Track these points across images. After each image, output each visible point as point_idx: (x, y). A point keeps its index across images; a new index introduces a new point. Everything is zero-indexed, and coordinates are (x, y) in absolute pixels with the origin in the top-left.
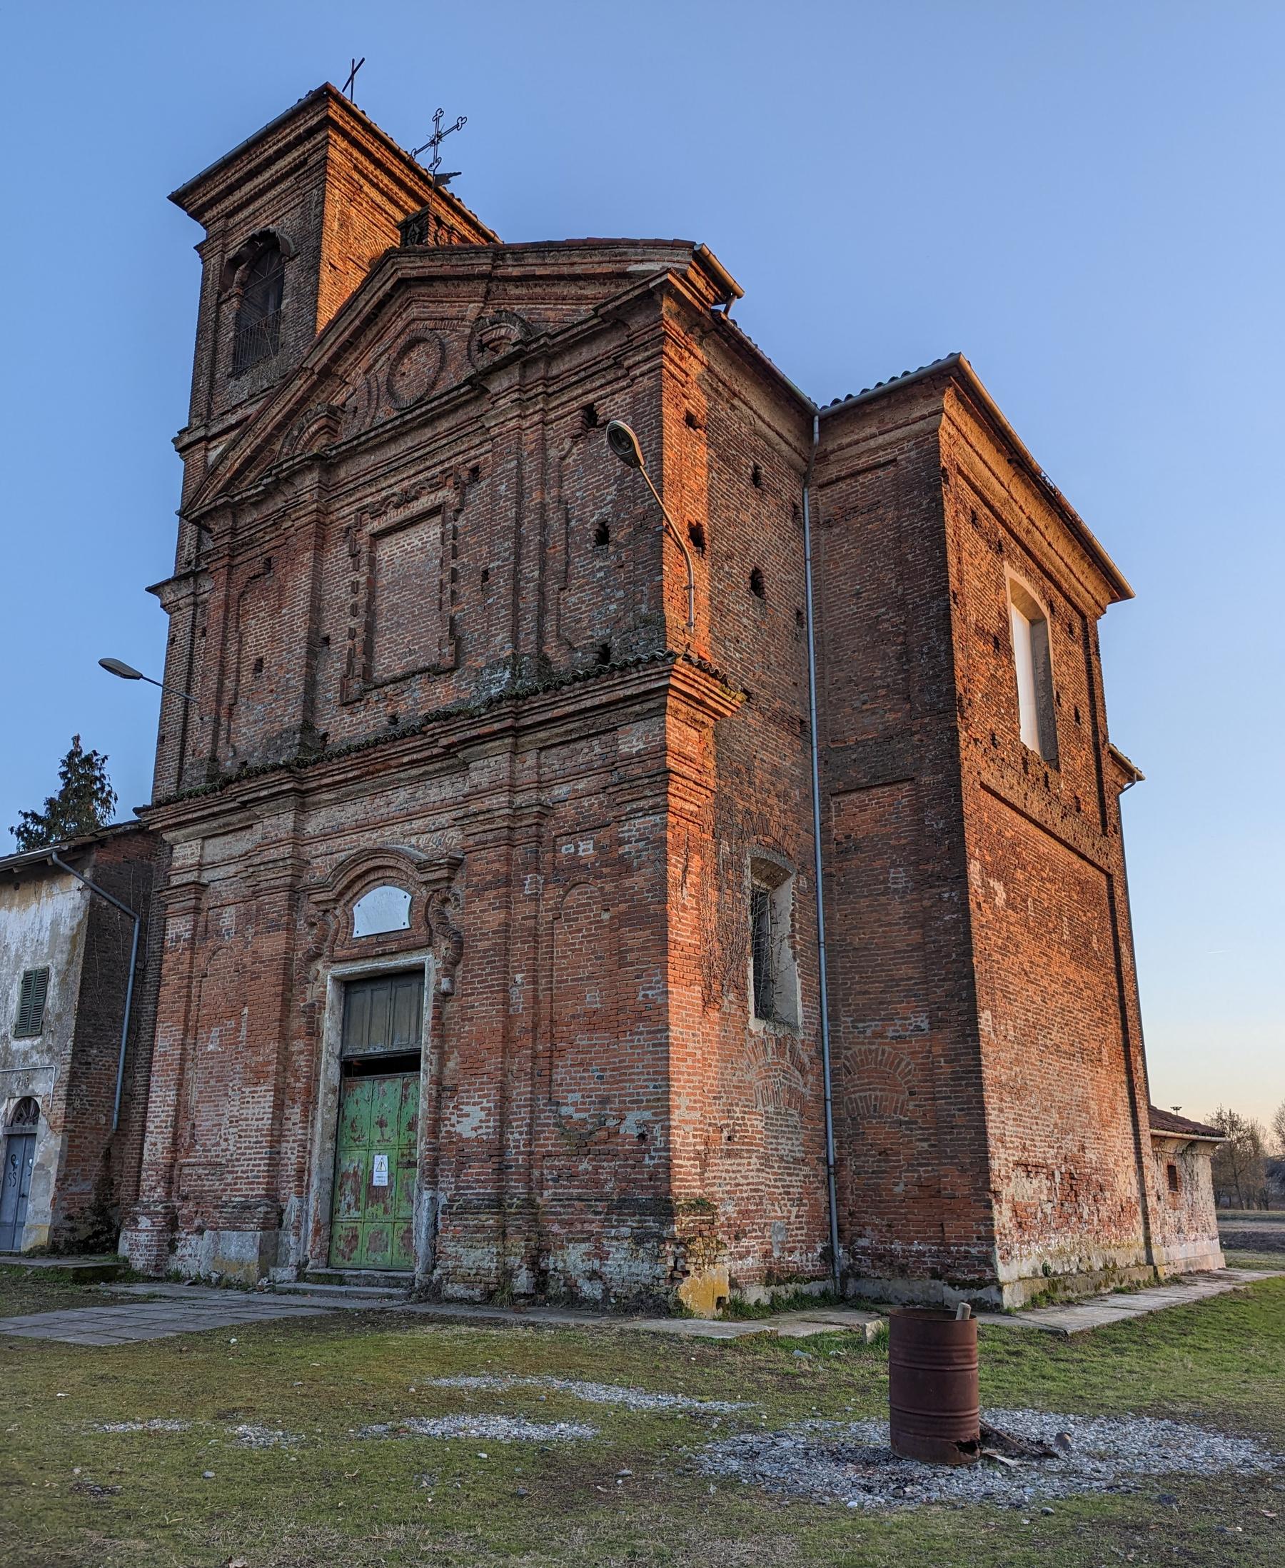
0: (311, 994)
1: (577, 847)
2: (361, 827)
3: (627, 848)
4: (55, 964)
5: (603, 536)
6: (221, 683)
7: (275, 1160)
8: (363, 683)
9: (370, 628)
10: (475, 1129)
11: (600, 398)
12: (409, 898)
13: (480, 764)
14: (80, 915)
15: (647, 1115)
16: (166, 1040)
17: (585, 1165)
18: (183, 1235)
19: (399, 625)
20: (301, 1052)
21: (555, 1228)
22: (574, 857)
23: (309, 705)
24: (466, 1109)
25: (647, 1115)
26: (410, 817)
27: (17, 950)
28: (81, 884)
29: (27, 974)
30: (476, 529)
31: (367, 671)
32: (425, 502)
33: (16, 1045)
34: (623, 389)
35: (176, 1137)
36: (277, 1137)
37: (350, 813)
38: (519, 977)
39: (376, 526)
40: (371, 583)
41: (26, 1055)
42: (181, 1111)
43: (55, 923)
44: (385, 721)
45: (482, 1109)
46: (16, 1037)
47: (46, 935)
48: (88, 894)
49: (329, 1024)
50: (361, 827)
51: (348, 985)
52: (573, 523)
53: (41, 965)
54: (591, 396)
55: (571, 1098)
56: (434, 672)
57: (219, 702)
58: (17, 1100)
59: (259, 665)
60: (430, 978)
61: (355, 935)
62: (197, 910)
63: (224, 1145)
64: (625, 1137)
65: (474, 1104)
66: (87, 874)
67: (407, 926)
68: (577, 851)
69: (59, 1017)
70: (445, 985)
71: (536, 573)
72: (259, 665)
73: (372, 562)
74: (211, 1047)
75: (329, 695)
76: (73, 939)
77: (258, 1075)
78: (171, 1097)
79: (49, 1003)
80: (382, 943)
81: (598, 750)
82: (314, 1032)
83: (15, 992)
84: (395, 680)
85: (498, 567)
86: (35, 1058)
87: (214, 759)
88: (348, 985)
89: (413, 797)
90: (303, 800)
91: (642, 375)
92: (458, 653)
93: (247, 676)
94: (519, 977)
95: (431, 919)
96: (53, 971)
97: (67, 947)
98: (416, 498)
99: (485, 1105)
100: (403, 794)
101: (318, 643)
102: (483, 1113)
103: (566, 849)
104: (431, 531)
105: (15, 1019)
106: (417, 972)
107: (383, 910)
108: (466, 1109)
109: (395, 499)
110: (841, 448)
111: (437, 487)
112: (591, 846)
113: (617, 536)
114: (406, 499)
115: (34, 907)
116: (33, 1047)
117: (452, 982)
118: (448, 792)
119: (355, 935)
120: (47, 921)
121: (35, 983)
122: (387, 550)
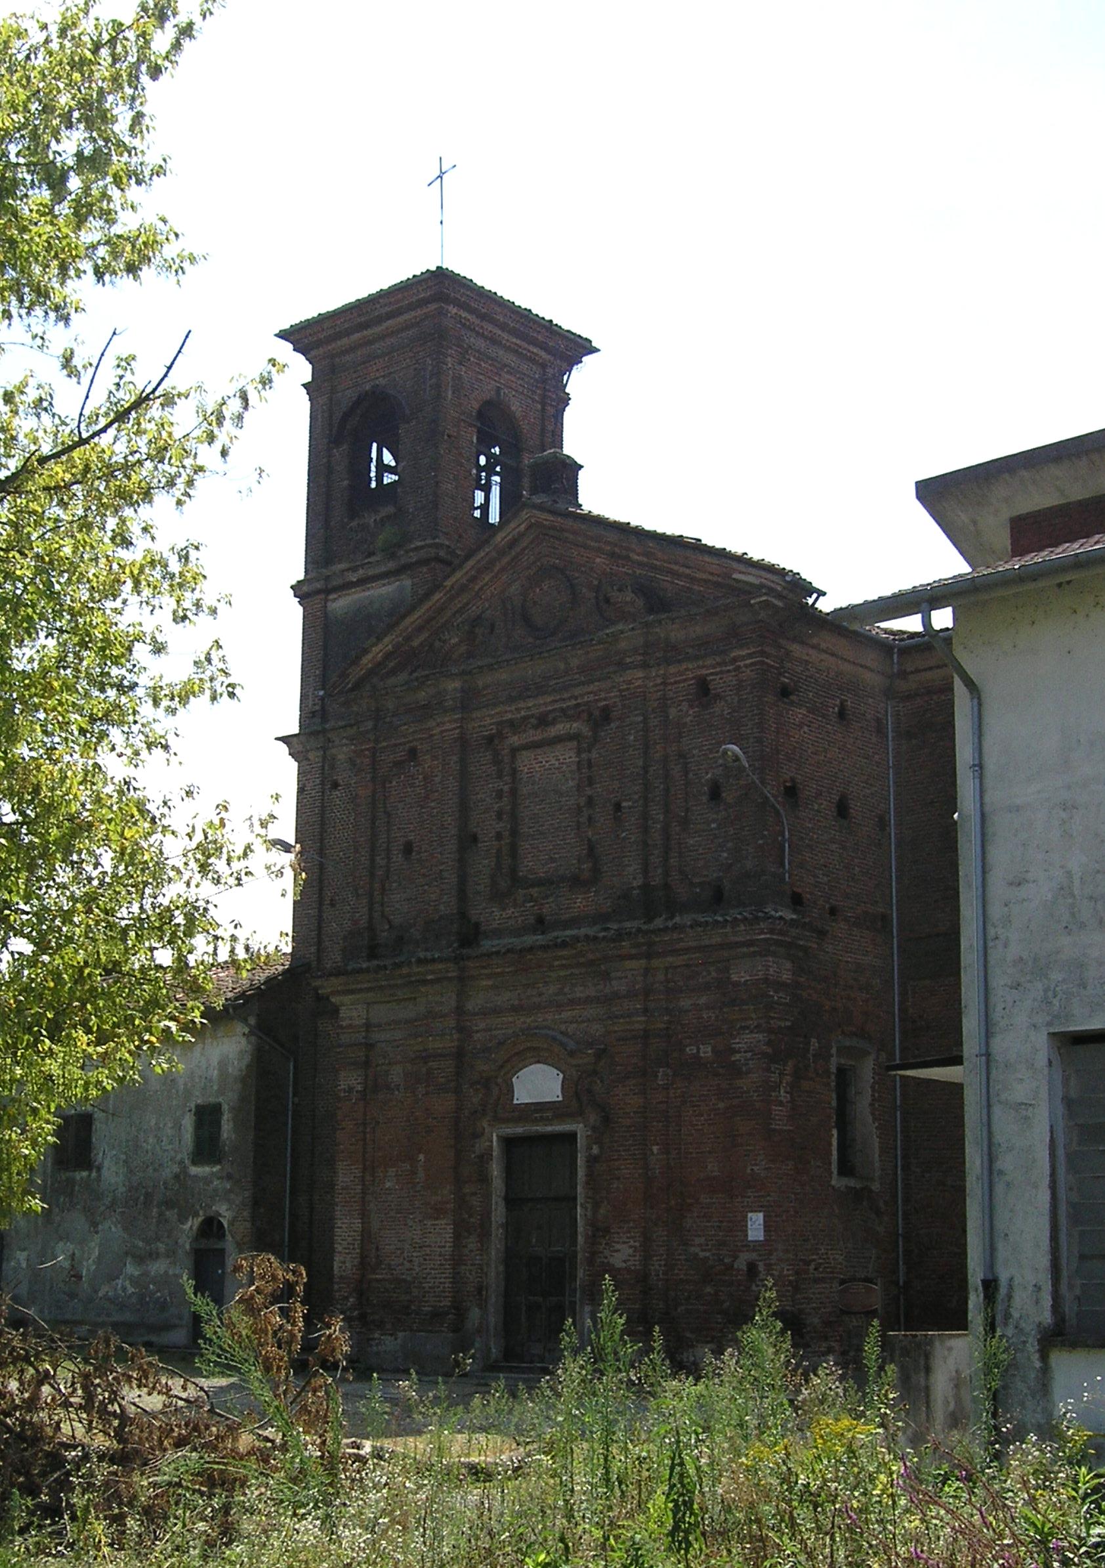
0: (480, 1146)
1: (698, 1049)
2: (515, 1009)
3: (738, 1056)
4: (228, 1102)
5: (715, 793)
6: (372, 861)
9: (514, 833)
10: (625, 1261)
11: (712, 674)
12: (561, 1076)
13: (619, 974)
14: (247, 1059)
15: (754, 1256)
16: (346, 1176)
17: (709, 1289)
18: (376, 1336)
20: (475, 1194)
21: (688, 1335)
22: (696, 1057)
23: (462, 895)
24: (618, 1246)
25: (754, 1256)
27: (185, 1084)
28: (246, 1030)
29: (197, 1106)
31: (513, 871)
32: (560, 728)
33: (194, 1170)
34: (729, 671)
35: (363, 1257)
38: (655, 1149)
39: (515, 740)
41: (207, 1180)
42: (366, 1235)
43: (223, 1065)
44: (532, 920)
45: (631, 1247)
46: (194, 1163)
48: (253, 1039)
49: (496, 1170)
51: (509, 1143)
52: (691, 775)
53: (212, 1100)
54: (704, 672)
55: (697, 1241)
56: (576, 882)
57: (372, 875)
58: (200, 1219)
59: (408, 849)
60: (581, 1142)
61: (515, 1102)
62: (367, 1064)
63: (407, 1265)
64: (738, 1270)
65: (624, 1243)
66: (252, 1021)
67: (560, 1099)
68: (698, 1052)
70: (595, 1150)
71: (661, 817)
72: (408, 849)
73: (514, 772)
74: (388, 1185)
75: (478, 888)
76: (244, 1080)
78: (357, 1224)
79: (225, 1135)
80: (539, 1109)
81: (714, 974)
82: (484, 1178)
83: (188, 1122)
84: (540, 883)
85: (630, 808)
87: (371, 928)
88: (509, 1143)
91: (746, 666)
92: (596, 870)
93: (398, 858)
94: (655, 1149)
95: (579, 1095)
96: (225, 1107)
98: (554, 722)
99: (632, 1243)
100: (553, 989)
101: (468, 840)
102: (631, 1251)
103: (691, 1050)
104: (566, 755)
106: (572, 1137)
107: (538, 1084)
108: (618, 1246)
109: (533, 721)
110: (917, 671)
112: (709, 1049)
113: (728, 796)
114: (543, 721)
116: (212, 1174)
117: (601, 1148)
118: (591, 992)
119: (515, 1102)
120: (215, 1062)
121: (207, 1116)
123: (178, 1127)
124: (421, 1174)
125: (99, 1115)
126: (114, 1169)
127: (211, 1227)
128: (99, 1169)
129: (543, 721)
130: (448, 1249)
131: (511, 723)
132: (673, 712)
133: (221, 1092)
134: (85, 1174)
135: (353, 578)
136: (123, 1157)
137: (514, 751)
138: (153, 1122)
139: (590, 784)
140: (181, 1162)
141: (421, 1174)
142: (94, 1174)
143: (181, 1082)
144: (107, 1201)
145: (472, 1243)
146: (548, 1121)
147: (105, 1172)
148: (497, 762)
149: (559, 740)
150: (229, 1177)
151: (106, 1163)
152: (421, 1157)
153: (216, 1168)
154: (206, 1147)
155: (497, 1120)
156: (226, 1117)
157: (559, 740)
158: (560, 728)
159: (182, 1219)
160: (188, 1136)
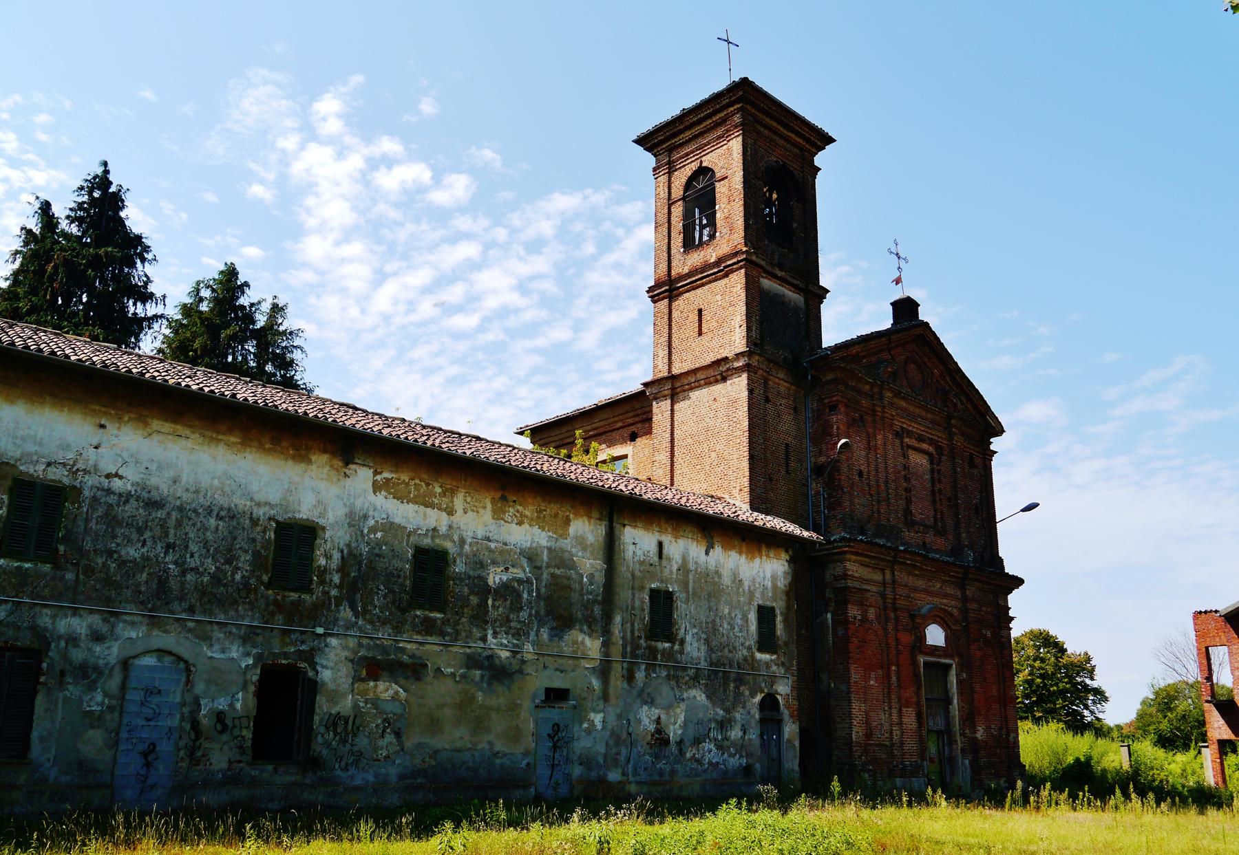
4: (779, 606)
29: (759, 606)
32: (924, 446)
33: (759, 656)
41: (767, 665)
43: (774, 578)
46: (760, 650)
47: (770, 584)
69: (786, 644)
76: (787, 593)
79: (779, 633)
83: (753, 617)
86: (774, 668)
96: (778, 612)
97: (784, 598)
105: (755, 637)
106: (949, 666)
115: (758, 560)
120: (768, 575)
121: (765, 614)
123: (745, 619)
125: (680, 596)
126: (695, 645)
127: (770, 703)
128: (682, 642)
133: (774, 599)
134: (667, 645)
135: (780, 274)
136: (704, 636)
138: (726, 611)
140: (749, 648)
142: (676, 647)
143: (746, 584)
144: (691, 672)
146: (940, 656)
147: (688, 648)
150: (783, 664)
151: (689, 638)
153: (774, 657)
154: (766, 641)
155: (922, 653)
156: (779, 619)
158: (924, 446)
159: (753, 695)
160: (753, 627)
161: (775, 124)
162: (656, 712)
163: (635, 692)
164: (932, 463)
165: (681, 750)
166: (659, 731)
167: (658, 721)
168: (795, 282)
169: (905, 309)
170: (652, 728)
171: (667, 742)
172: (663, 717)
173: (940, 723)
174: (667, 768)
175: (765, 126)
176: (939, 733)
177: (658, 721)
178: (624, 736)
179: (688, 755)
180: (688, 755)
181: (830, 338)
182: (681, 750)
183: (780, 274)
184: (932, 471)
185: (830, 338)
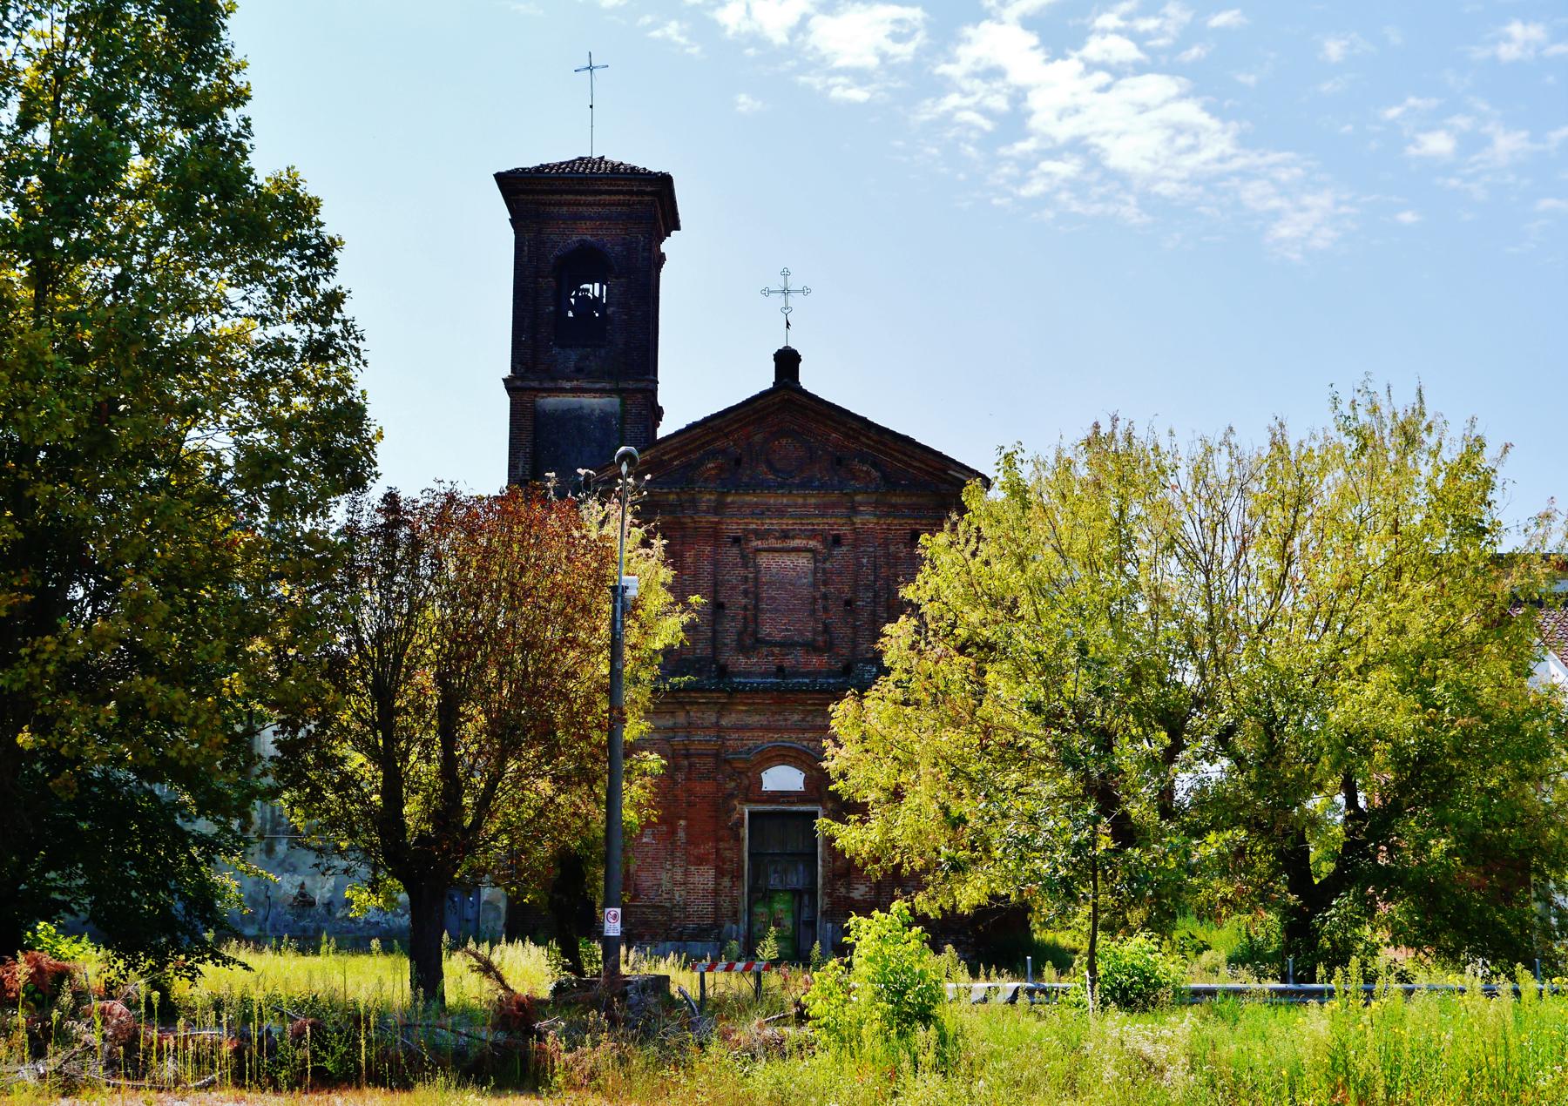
7: (717, 906)
8: (751, 641)
19: (777, 611)
26: (804, 730)
30: (840, 574)
31: (755, 632)
36: (716, 892)
37: (754, 720)
40: (756, 578)
44: (774, 668)
50: (766, 729)
56: (811, 647)
73: (756, 566)
77: (700, 861)
82: (738, 839)
84: (776, 644)
89: (803, 720)
90: (722, 709)
98: (793, 538)
100: (796, 717)
104: (803, 562)
111: (809, 538)
114: (785, 535)
122: (764, 560)
124: (681, 834)
129: (785, 535)
130: (711, 886)
131: (755, 532)
132: (892, 549)
135: (568, 385)
137: (758, 550)
139: (825, 584)
141: (681, 834)
145: (726, 882)
146: (793, 803)
148: (743, 557)
149: (797, 550)
152: (682, 822)
155: (748, 801)
157: (797, 550)
161: (570, 197)
162: (298, 879)
163: (274, 863)
164: (816, 561)
165: (329, 911)
166: (302, 895)
167: (302, 886)
168: (598, 386)
169: (787, 361)
170: (295, 892)
171: (313, 903)
172: (308, 883)
173: (796, 879)
174: (313, 925)
175: (560, 204)
176: (797, 893)
177: (302, 886)
178: (262, 898)
179: (338, 915)
180: (338, 915)
181: (659, 436)
182: (329, 911)
183: (568, 385)
184: (815, 571)
185: (659, 436)
